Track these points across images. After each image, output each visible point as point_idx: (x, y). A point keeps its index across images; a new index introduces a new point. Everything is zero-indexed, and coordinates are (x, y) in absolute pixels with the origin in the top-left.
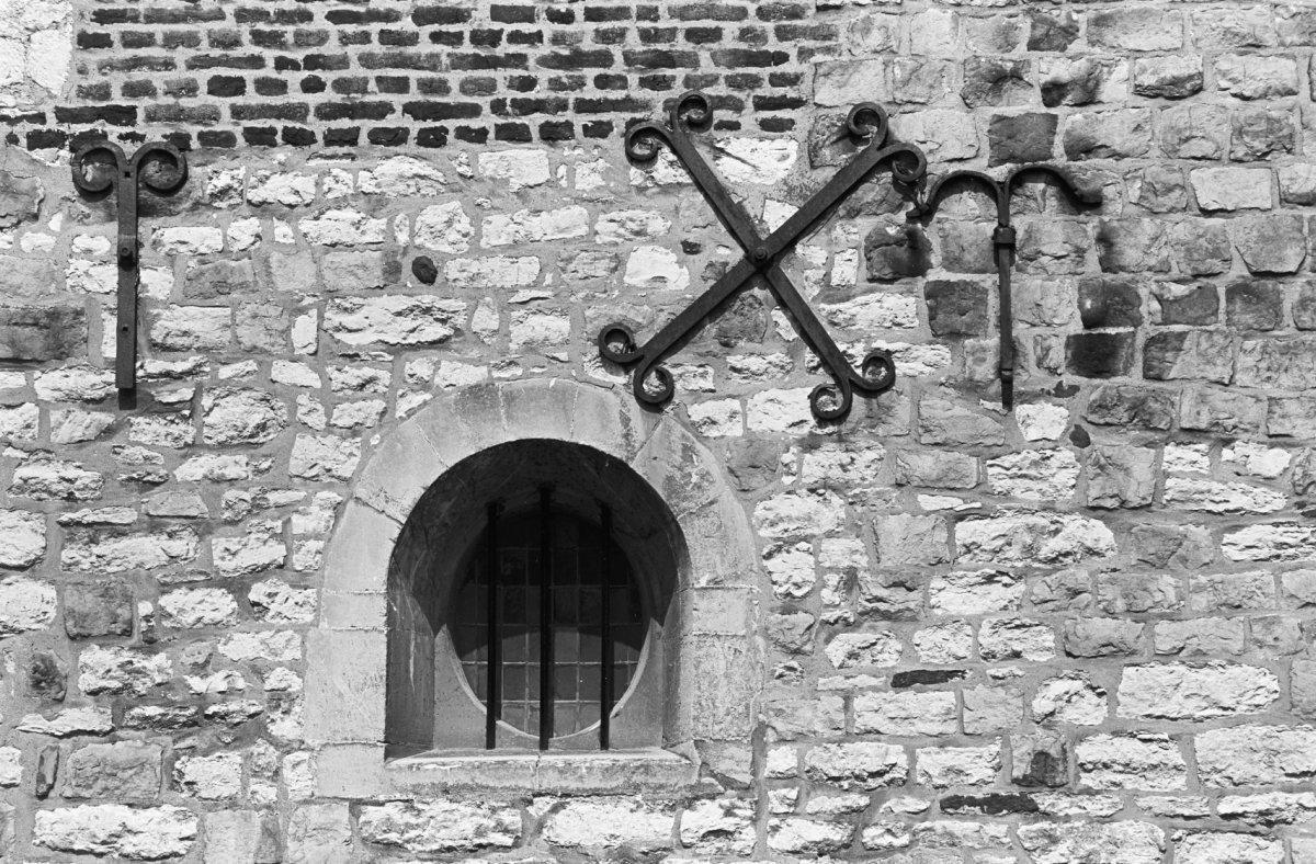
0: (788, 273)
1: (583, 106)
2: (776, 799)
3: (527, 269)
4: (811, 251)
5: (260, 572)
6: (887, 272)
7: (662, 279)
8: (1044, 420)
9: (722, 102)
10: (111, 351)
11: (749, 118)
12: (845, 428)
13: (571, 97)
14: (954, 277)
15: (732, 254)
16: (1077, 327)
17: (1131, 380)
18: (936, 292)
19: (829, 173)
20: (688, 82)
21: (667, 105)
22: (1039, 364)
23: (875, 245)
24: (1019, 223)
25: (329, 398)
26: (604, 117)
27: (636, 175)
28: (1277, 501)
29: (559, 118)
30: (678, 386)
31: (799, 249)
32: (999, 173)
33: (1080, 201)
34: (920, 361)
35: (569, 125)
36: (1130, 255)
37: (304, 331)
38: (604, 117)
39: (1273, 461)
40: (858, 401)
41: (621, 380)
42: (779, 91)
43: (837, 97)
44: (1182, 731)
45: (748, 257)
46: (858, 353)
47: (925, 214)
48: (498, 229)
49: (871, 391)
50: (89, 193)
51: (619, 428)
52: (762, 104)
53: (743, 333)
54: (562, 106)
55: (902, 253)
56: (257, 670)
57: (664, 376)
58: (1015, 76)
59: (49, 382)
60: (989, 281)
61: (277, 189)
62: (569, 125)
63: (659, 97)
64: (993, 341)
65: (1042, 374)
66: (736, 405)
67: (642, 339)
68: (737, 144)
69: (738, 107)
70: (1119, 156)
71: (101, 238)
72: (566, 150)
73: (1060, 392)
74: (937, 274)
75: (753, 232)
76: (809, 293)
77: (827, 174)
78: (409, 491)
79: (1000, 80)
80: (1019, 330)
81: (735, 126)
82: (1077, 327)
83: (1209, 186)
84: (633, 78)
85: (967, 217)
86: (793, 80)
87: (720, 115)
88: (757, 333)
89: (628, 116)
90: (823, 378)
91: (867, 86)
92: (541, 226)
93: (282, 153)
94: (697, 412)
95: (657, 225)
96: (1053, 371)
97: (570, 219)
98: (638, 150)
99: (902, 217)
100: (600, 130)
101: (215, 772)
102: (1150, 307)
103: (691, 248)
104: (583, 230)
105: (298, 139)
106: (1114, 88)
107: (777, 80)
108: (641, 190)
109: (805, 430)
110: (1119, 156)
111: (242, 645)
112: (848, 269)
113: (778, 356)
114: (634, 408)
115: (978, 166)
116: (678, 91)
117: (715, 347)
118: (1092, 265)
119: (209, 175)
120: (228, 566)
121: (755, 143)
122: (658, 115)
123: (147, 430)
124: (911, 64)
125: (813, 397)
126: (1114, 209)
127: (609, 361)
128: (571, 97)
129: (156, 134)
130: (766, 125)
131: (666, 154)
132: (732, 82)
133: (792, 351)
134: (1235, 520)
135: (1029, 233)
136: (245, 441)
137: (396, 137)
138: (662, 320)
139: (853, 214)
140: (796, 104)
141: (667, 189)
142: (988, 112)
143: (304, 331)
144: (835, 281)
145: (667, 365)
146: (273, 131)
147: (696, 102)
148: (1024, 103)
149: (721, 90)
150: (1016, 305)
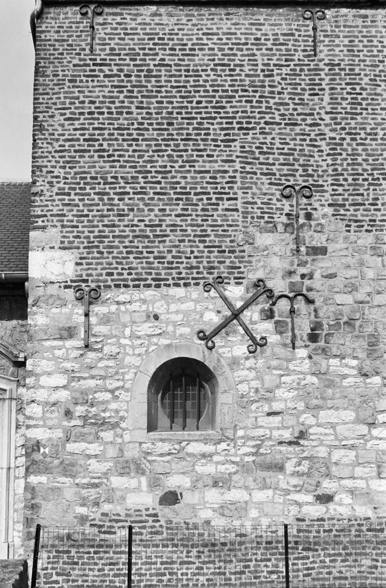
0: (242, 318)
1: (193, 279)
2: (239, 442)
3: (180, 317)
5: (117, 388)
6: (265, 318)
7: (212, 319)
8: (302, 353)
9: (226, 278)
10: (83, 336)
11: (232, 281)
12: (256, 354)
13: (190, 276)
14: (281, 319)
15: (229, 313)
16: (310, 331)
17: (322, 343)
18: (277, 322)
19: (252, 294)
20: (218, 273)
21: (213, 279)
22: (301, 339)
23: (262, 311)
24: (295, 306)
25: (133, 347)
26: (198, 281)
27: (206, 294)
28: (355, 372)
29: (188, 281)
30: (216, 344)
31: (244, 312)
32: (291, 295)
33: (309, 301)
34: (273, 338)
35: (190, 283)
36: (321, 314)
37: (128, 332)
38: (198, 281)
39: (355, 363)
40: (258, 347)
41: (203, 342)
42: (239, 275)
43: (253, 277)
44: (333, 426)
45: (232, 314)
46: (258, 337)
47: (274, 304)
48: (173, 307)
49: (261, 346)
50: (79, 299)
51: (202, 354)
52: (235, 278)
53: (231, 332)
54: (189, 278)
55: (269, 313)
56: (117, 411)
57: (212, 342)
58: (294, 272)
59: (69, 343)
60: (289, 320)
61: (121, 298)
62: (190, 283)
63: (211, 277)
64: (290, 334)
65: (302, 342)
66: (230, 349)
67: (207, 333)
68: (229, 287)
69: (230, 279)
70: (318, 291)
71: (81, 310)
72: (189, 289)
73: (306, 346)
74: (277, 318)
75: (233, 308)
76: (247, 323)
77: (250, 295)
78: (152, 369)
79: (291, 273)
80: (296, 331)
81: (229, 283)
82: (310, 331)
83: (339, 299)
84: (205, 272)
85: (283, 305)
86: (242, 273)
87: (226, 281)
88: (235, 332)
89: (204, 281)
90: (250, 342)
91: (260, 274)
92: (184, 307)
93: (123, 290)
94: (221, 351)
95: (211, 307)
96: (304, 341)
97: (190, 305)
98: (206, 289)
99: (268, 305)
100: (197, 284)
101: (108, 435)
102: (326, 326)
103: (219, 312)
104: (193, 308)
105: (126, 286)
106: (317, 275)
107: (239, 273)
108: (207, 298)
109: (246, 355)
110: (318, 291)
111: (113, 406)
112: (256, 316)
113: (240, 338)
114: (206, 350)
115: (286, 293)
116: (216, 275)
117: (224, 335)
118: (312, 317)
119: (106, 295)
120: (110, 387)
121: (234, 287)
122: (211, 281)
123: (91, 355)
124: (270, 269)
125: (248, 347)
126: (318, 304)
127: (201, 339)
128: (190, 276)
129: (93, 285)
130: (236, 283)
131: (213, 290)
132: (228, 273)
133: (243, 336)
134: (345, 377)
135: (298, 310)
136: (113, 357)
137: (149, 286)
138: (212, 329)
139: (257, 304)
140: (243, 278)
141: (213, 298)
142: (288, 280)
143: (128, 332)
144: (253, 320)
145: (213, 339)
146: (120, 285)
147: (220, 277)
149: (226, 275)
150: (295, 326)
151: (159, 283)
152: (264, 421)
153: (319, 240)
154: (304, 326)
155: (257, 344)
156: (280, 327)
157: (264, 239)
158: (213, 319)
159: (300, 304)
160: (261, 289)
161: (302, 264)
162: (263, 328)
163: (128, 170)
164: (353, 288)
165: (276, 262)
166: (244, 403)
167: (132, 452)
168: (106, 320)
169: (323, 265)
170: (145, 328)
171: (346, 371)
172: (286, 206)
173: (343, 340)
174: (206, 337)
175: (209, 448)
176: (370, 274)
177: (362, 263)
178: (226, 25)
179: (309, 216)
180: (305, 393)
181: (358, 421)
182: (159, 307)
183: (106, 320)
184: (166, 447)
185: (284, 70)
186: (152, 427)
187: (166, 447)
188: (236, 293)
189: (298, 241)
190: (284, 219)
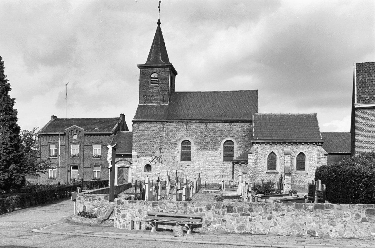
8: (160, 164)
33: (161, 158)
34: (157, 162)
43: (155, 155)
71: (137, 159)
78: (145, 165)
85: (159, 159)
91: (156, 155)
101: (140, 172)
119: (140, 157)
148: (160, 156)
152: (156, 171)
153: (163, 151)
154: (161, 161)
155: (156, 163)
157: (157, 151)
158: (151, 160)
159: (160, 158)
160: (156, 157)
162: (156, 161)
164: (166, 157)
165: (158, 154)
166: (154, 169)
167: (142, 174)
168: (140, 160)
169: (163, 154)
170: (144, 161)
173: (165, 163)
175: (150, 174)
178: (154, 126)
179: (162, 149)
180: (160, 168)
182: (145, 159)
183: (140, 160)
184: (146, 174)
186: (145, 171)
187: (146, 174)
188: (154, 157)
189: (160, 151)
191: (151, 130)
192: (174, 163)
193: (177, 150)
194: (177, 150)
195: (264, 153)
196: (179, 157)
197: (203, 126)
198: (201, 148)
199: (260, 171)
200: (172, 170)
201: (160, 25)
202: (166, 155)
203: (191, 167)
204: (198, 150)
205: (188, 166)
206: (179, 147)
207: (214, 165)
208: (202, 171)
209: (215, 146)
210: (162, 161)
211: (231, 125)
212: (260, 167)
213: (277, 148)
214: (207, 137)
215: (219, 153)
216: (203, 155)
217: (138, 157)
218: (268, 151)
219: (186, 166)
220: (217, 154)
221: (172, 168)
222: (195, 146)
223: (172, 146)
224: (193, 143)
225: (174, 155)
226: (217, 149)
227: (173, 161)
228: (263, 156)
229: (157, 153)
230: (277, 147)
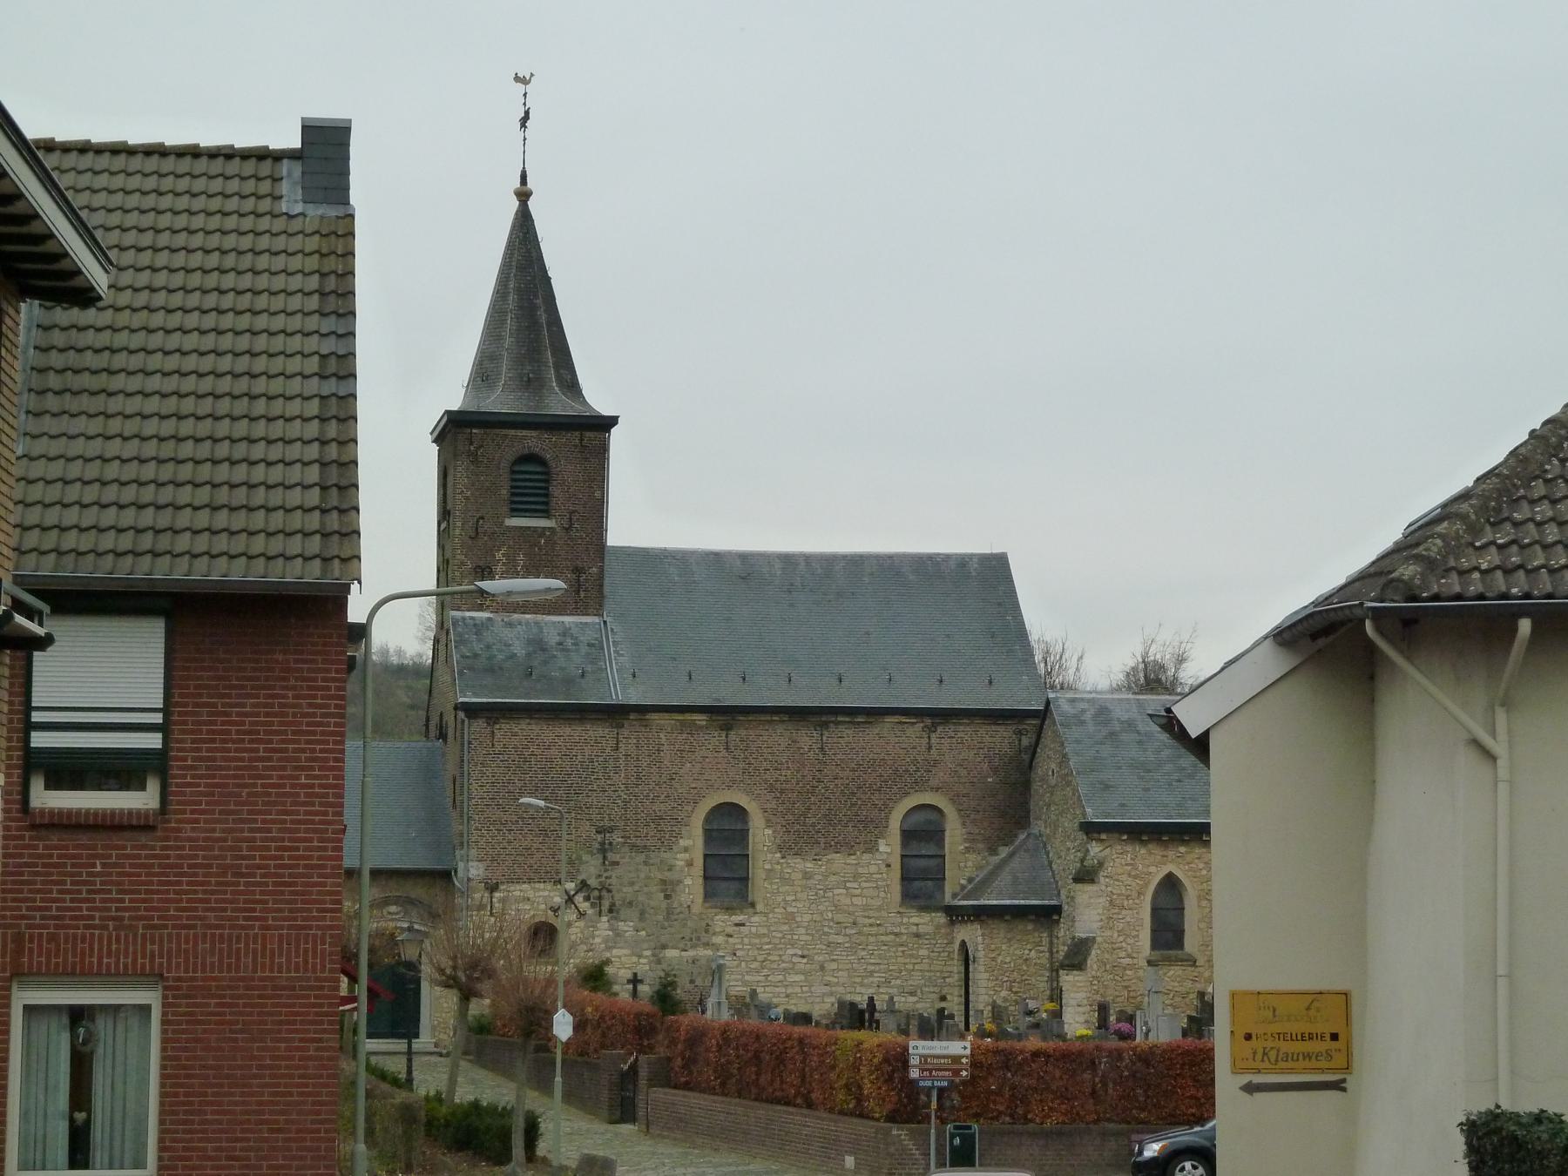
4: (576, 897)
8: (604, 919)
33: (609, 891)
34: (590, 912)
39: (632, 924)
43: (580, 878)
79: (600, 876)
92: (541, 893)
97: (546, 893)
112: (581, 899)
119: (502, 887)
151: (530, 881)
153: (616, 858)
154: (606, 904)
155: (582, 915)
156: (593, 905)
157: (585, 857)
159: (604, 893)
160: (584, 885)
161: (606, 871)
162: (584, 906)
163: (515, 818)
164: (632, 884)
166: (573, 946)
169: (615, 873)
171: (626, 929)
172: (599, 837)
173: (624, 912)
174: (555, 910)
176: (642, 875)
177: (637, 870)
178: (568, 730)
179: (611, 844)
181: (633, 954)
182: (531, 894)
185: (601, 759)
188: (571, 886)
189: (605, 858)
190: (597, 846)
191: (554, 751)
192: (669, 912)
193: (686, 850)
194: (686, 850)
195: (1136, 877)
196: (692, 886)
197: (807, 738)
198: (797, 840)
199: (1123, 954)
200: (664, 947)
201: (532, 204)
202: (630, 873)
203: (754, 930)
204: (785, 849)
205: (737, 928)
206: (693, 842)
207: (861, 920)
208: (806, 952)
209: (866, 831)
210: (613, 905)
211: (933, 735)
212: (1121, 939)
213: (1189, 858)
214: (827, 789)
215: (883, 867)
216: (807, 876)
217: (492, 888)
218: (1152, 869)
219: (730, 930)
220: (873, 869)
221: (663, 939)
222: (769, 832)
223: (666, 829)
224: (757, 823)
225: (668, 875)
226: (871, 848)
227: (664, 905)
228: (1134, 894)
229: (591, 869)
230: (1187, 853)
